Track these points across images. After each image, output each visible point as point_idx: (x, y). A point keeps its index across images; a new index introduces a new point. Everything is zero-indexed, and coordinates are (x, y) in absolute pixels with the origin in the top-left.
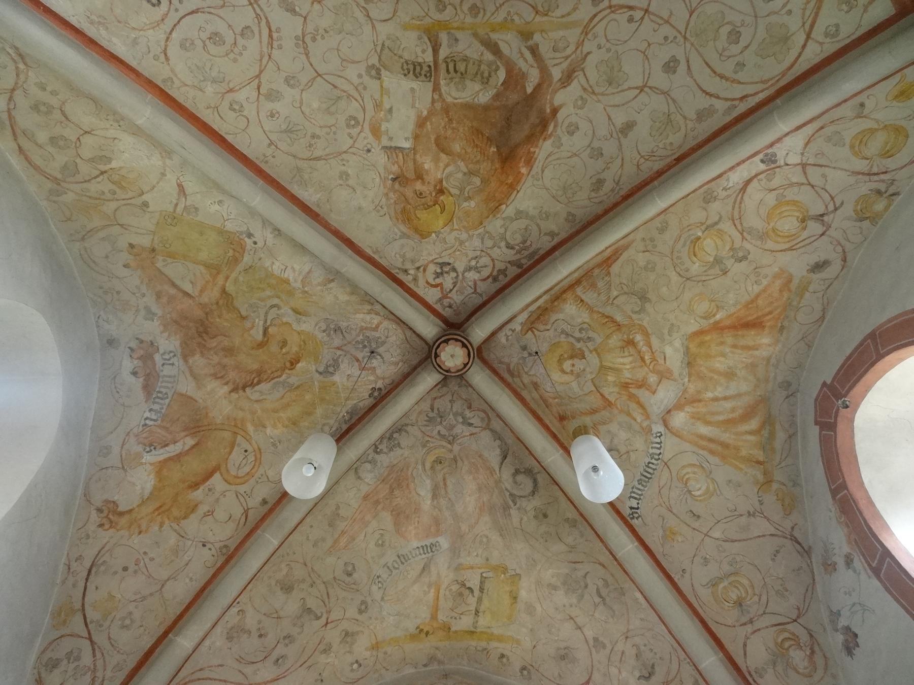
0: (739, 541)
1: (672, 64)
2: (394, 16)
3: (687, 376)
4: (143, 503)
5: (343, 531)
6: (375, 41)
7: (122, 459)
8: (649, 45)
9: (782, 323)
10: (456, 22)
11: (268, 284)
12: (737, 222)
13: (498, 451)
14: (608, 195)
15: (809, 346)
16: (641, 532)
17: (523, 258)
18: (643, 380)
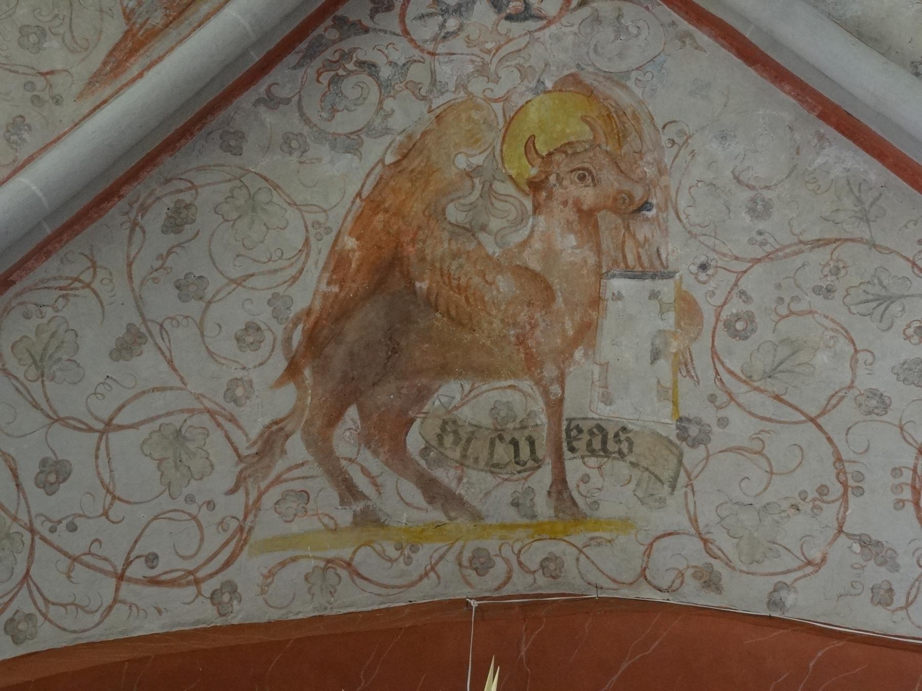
1: (52, 478)
2: (651, 544)
6: (690, 495)
8: (105, 514)
10: (517, 540)
17: (334, 42)
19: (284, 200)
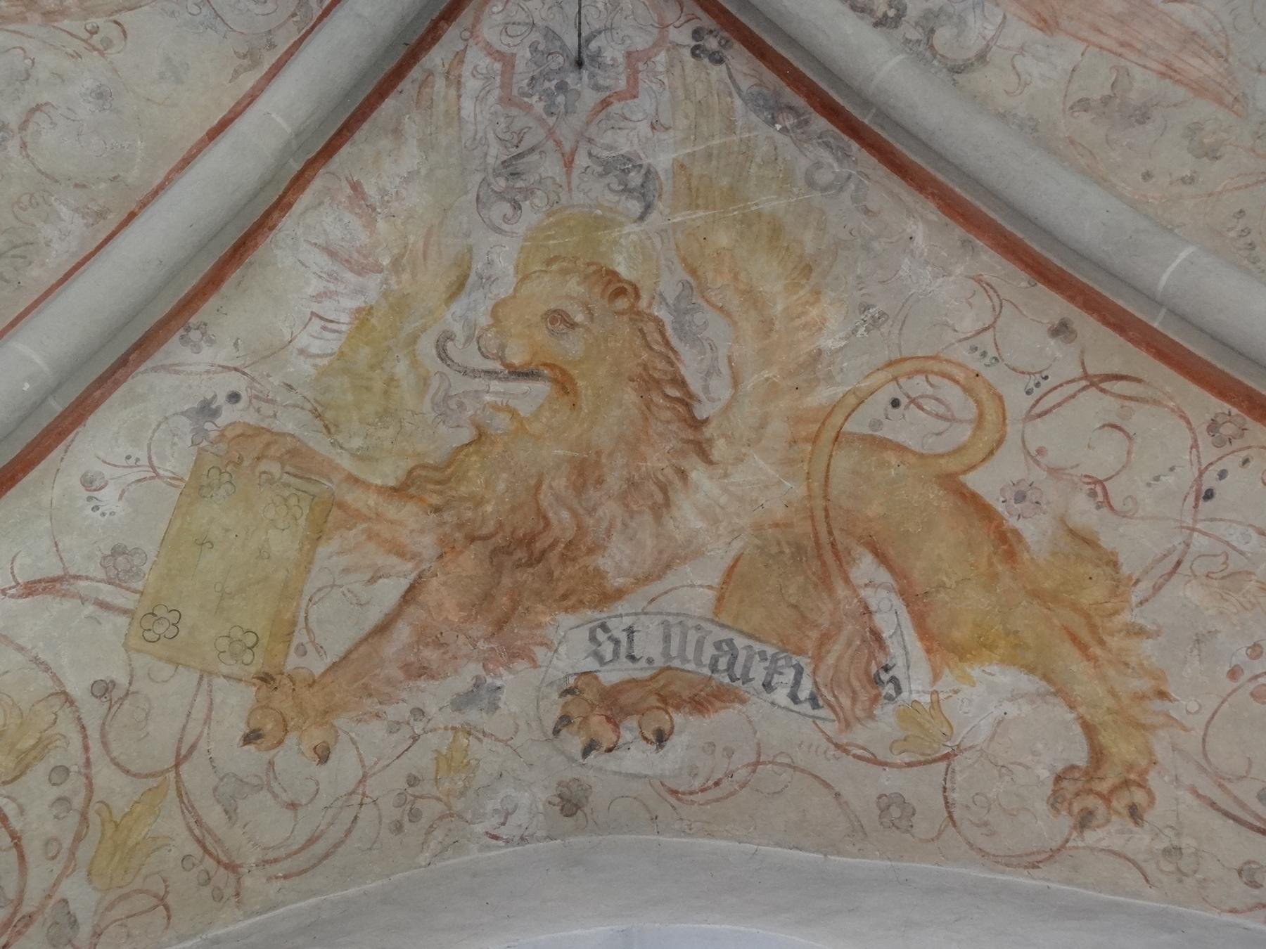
4: (1061, 691)
5: (1163, 75)
7: (920, 763)
11: (372, 367)
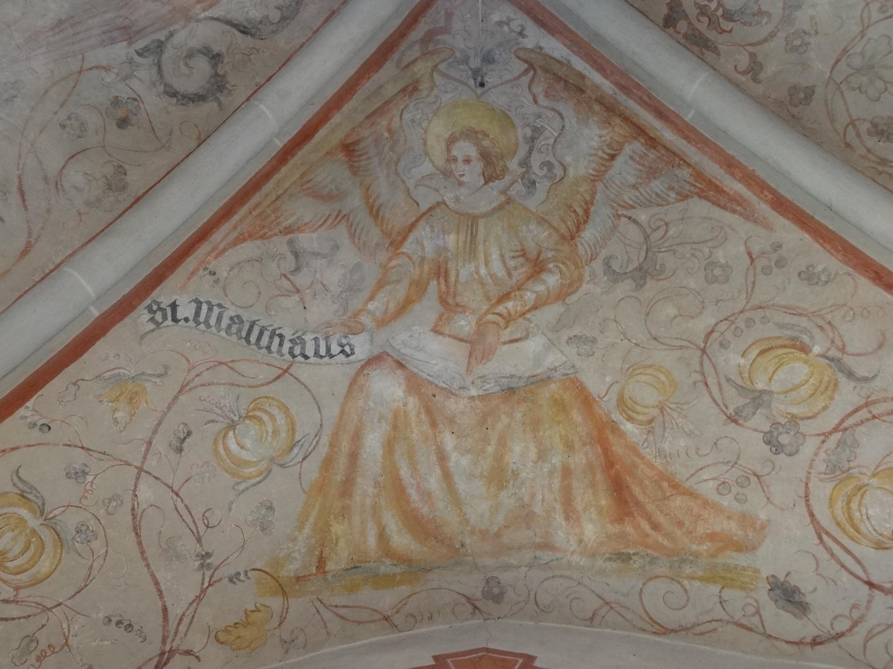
0: (140, 544)
3: (481, 392)
9: (634, 554)
12: (864, 414)
13: (255, 14)
14: (869, 156)
15: (592, 619)
16: (121, 331)
17: (690, 23)
18: (457, 305)
19: (859, 41)
